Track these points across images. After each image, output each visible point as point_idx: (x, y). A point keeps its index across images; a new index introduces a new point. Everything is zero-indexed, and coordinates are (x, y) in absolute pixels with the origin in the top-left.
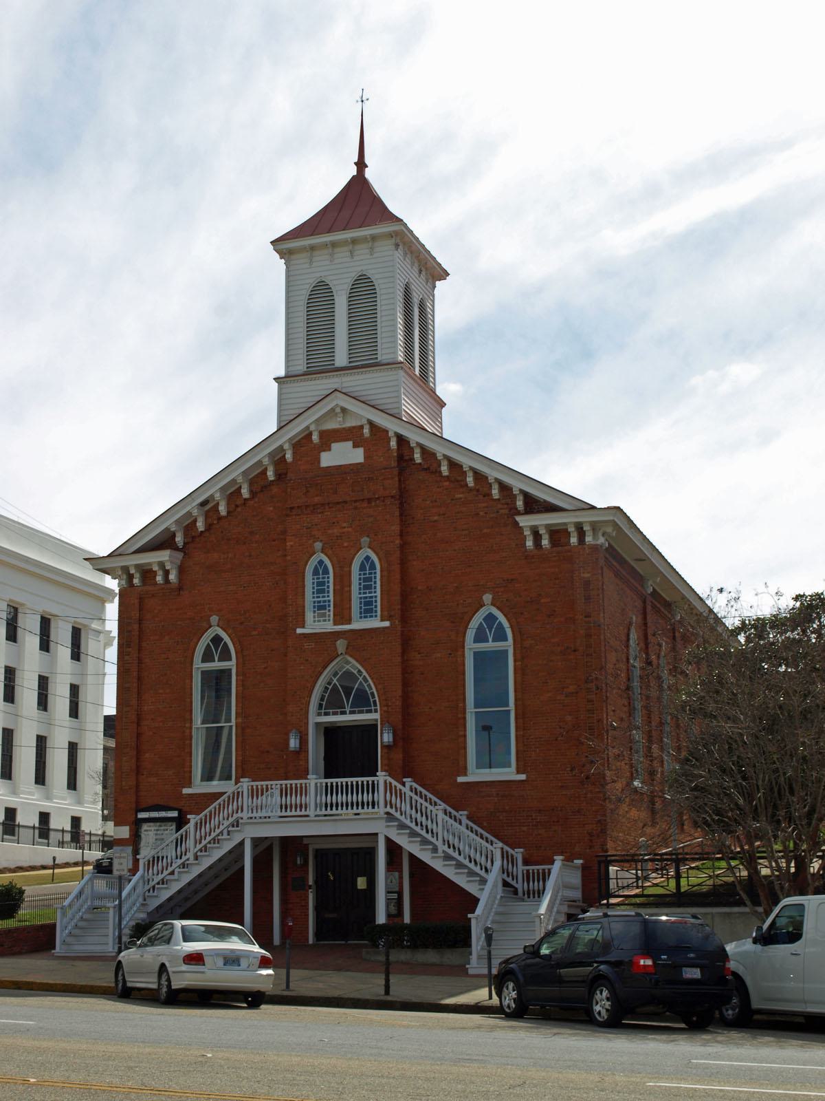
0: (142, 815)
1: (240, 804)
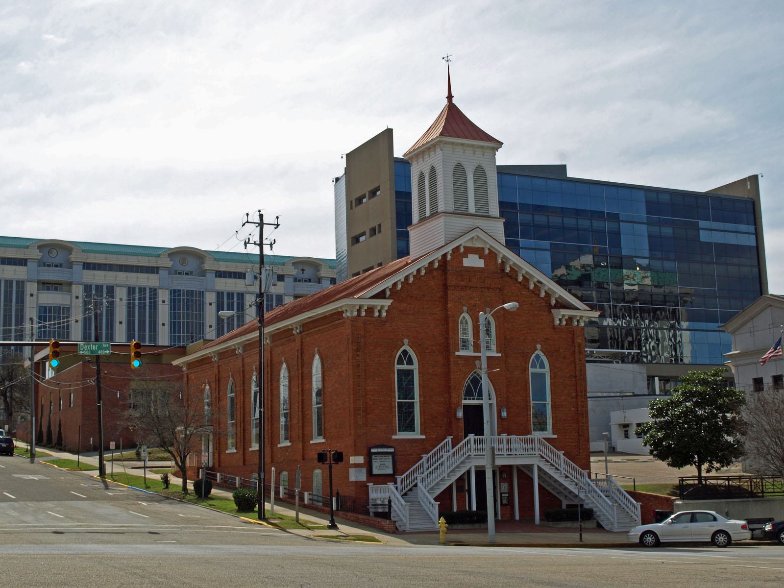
0: (373, 450)
1: (469, 448)
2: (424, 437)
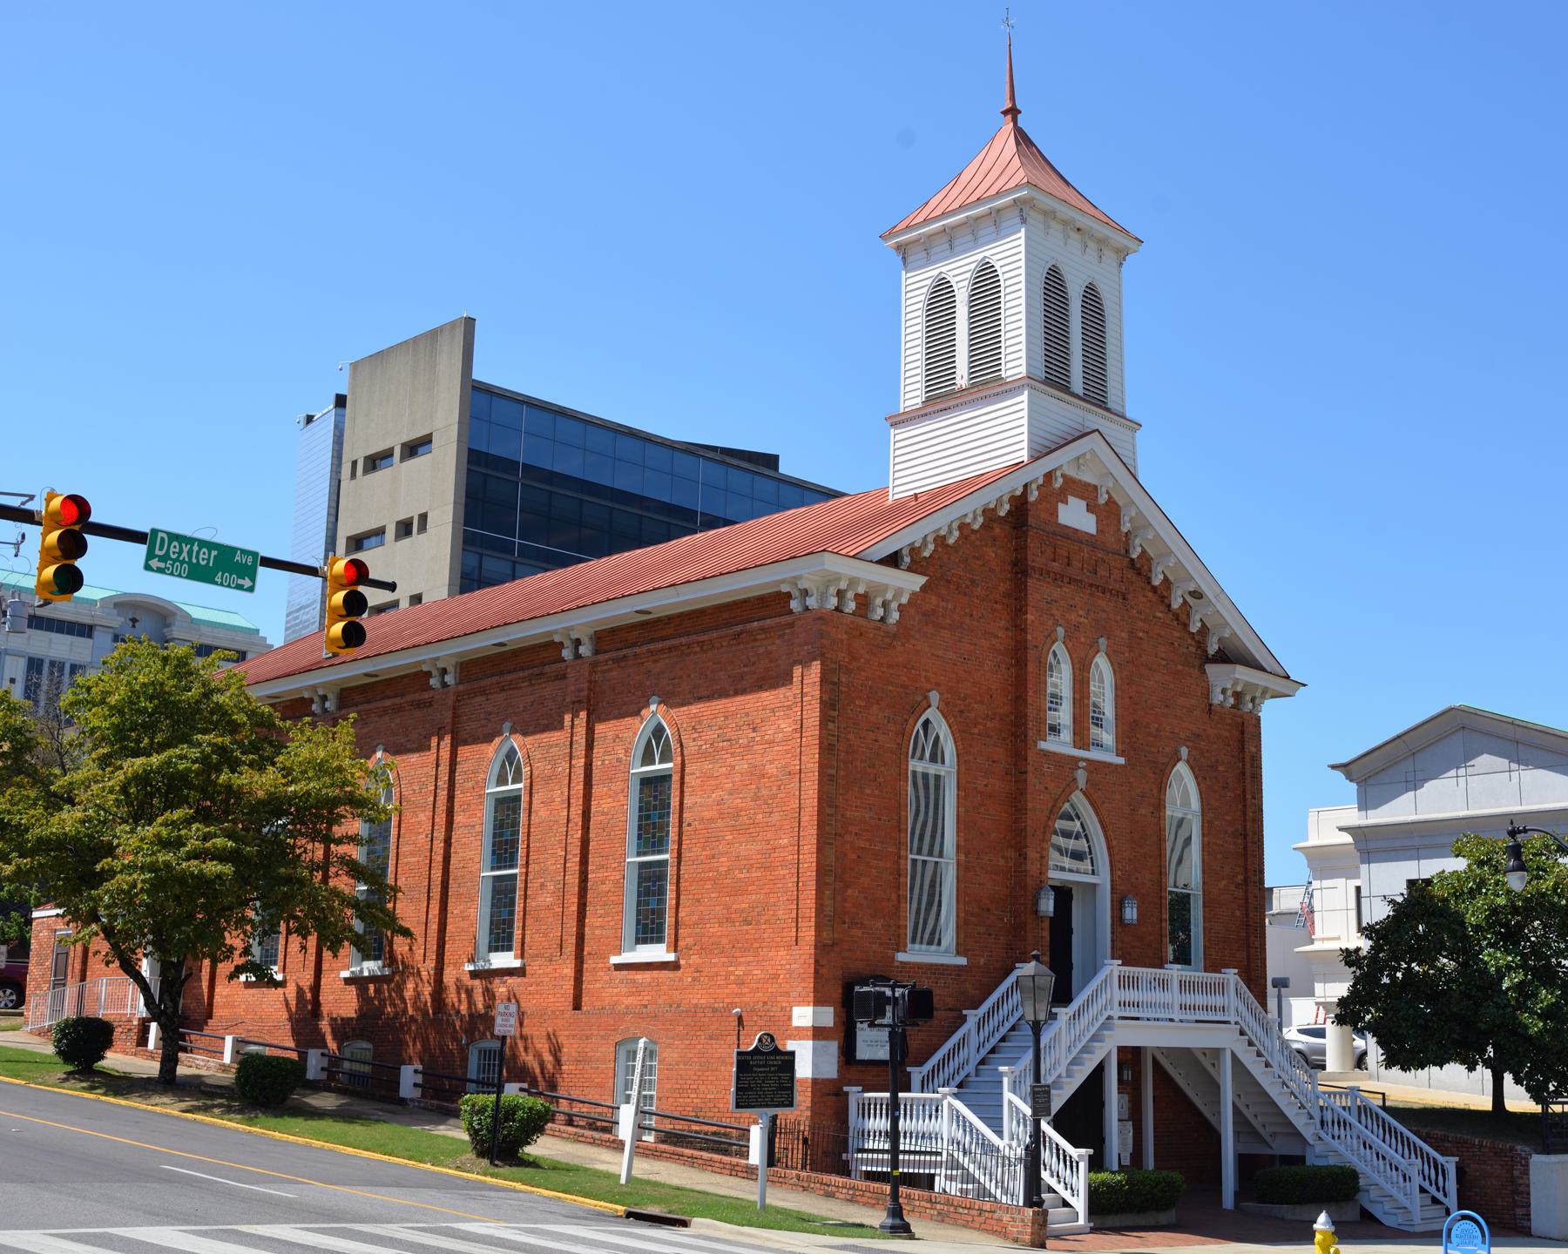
2: (963, 961)
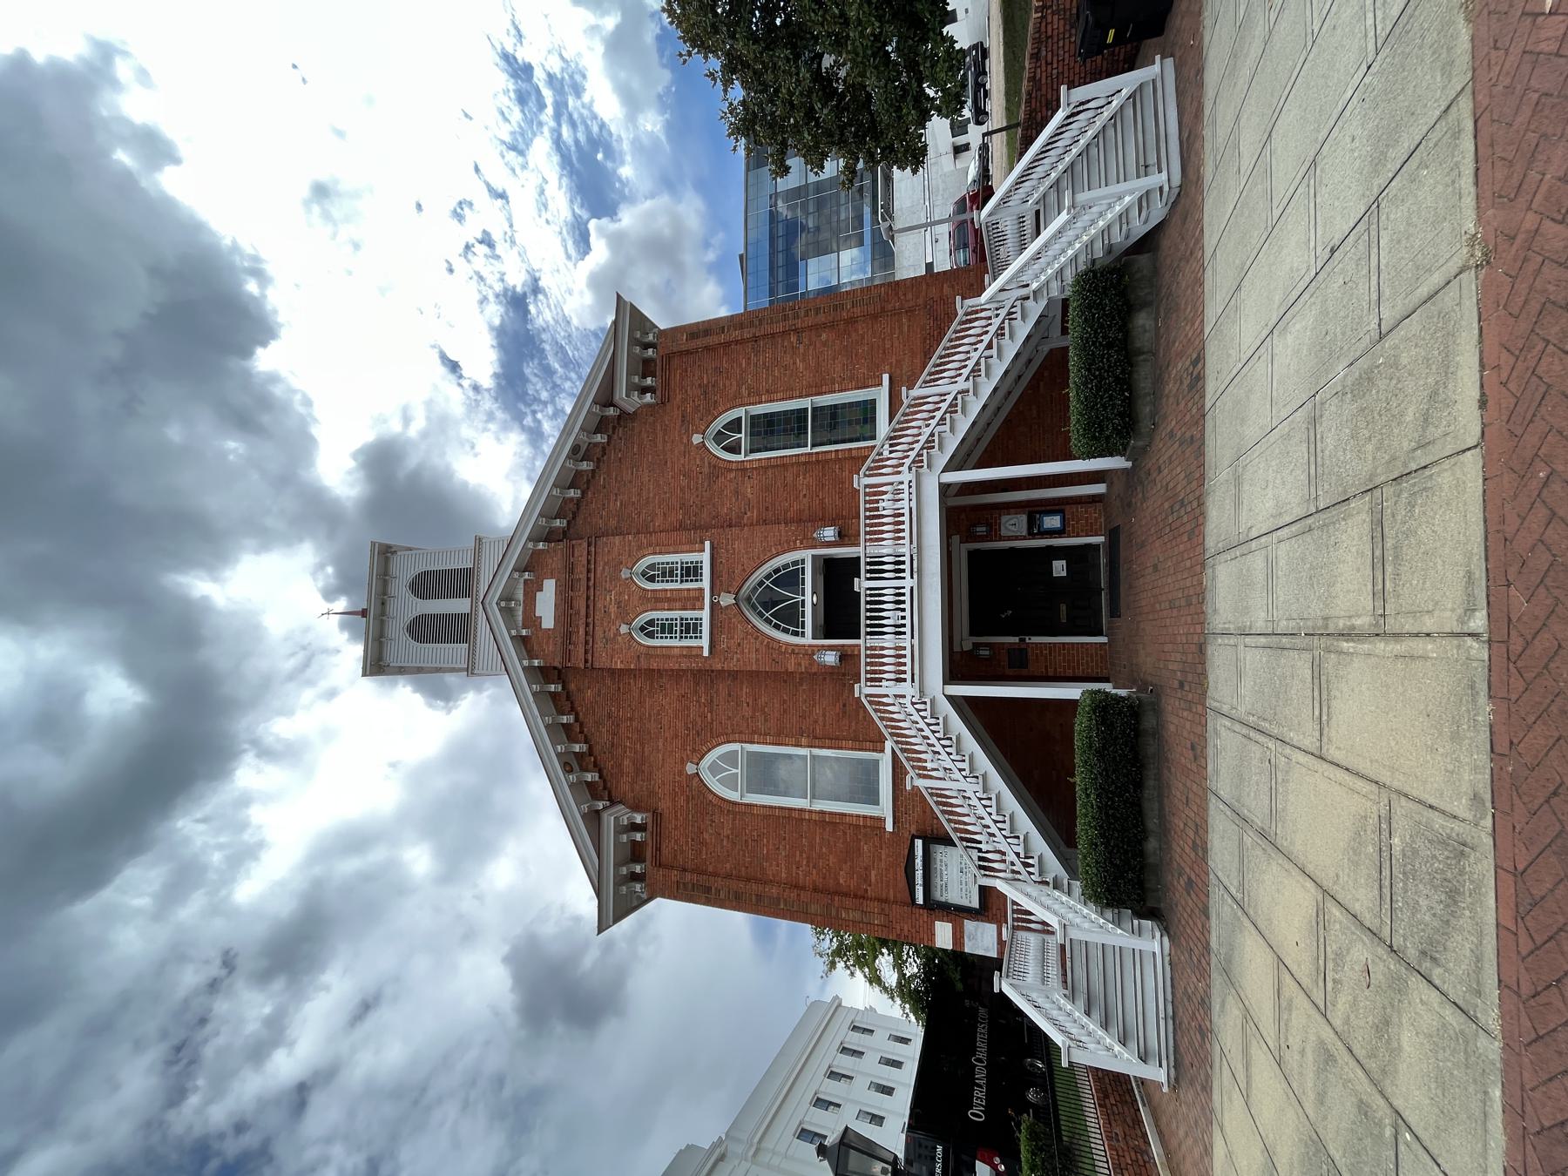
0: (920, 901)
